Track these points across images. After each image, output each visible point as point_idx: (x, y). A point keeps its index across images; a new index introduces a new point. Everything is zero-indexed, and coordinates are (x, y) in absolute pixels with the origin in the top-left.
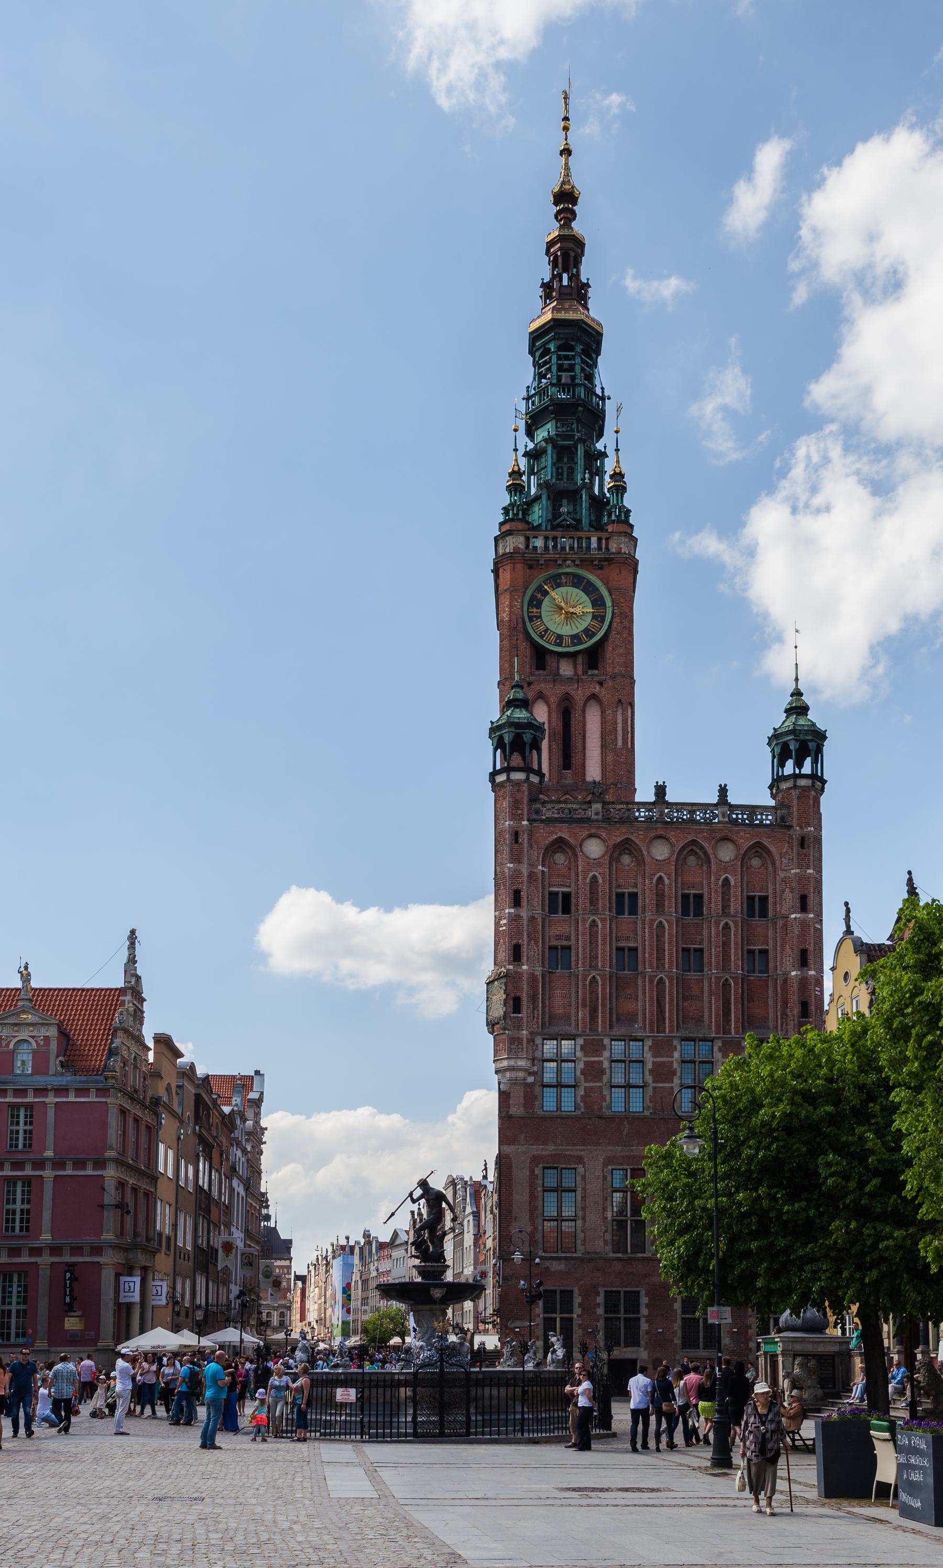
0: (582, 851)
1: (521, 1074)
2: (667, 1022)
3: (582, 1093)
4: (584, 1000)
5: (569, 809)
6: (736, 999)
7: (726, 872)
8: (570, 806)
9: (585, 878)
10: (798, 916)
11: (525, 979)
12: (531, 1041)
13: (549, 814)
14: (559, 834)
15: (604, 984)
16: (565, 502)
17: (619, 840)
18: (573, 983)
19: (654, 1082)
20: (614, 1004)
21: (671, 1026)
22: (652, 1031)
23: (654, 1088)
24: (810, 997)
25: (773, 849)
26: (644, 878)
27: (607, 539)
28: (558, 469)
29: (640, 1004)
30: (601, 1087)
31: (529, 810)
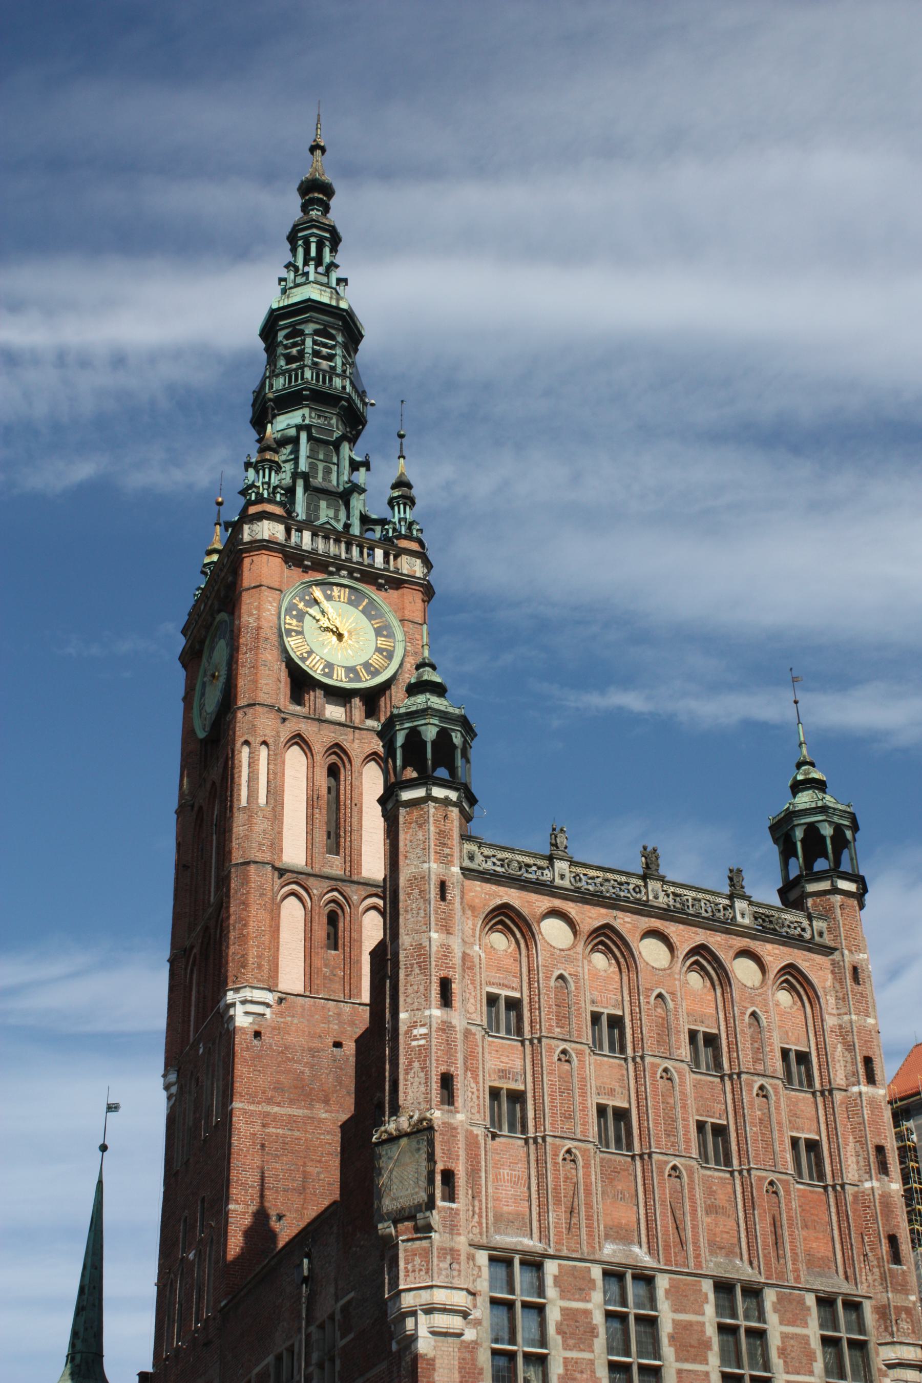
0: (541, 932)
1: (454, 1322)
2: (691, 1248)
3: (561, 1371)
4: (556, 1189)
5: (519, 862)
6: (790, 1218)
7: (753, 1004)
8: (520, 858)
9: (548, 978)
10: (864, 1089)
11: (461, 1137)
12: (471, 1258)
13: (489, 866)
14: (505, 900)
15: (587, 1166)
16: (323, 504)
17: (597, 924)
18: (533, 1157)
19: (678, 1359)
20: (600, 1206)
21: (697, 1256)
22: (668, 1262)
23: (679, 1372)
24: (897, 1226)
25: (815, 981)
26: (635, 991)
27: (396, 558)
28: (311, 464)
29: (642, 1211)
30: (591, 1362)
31: (461, 851)
